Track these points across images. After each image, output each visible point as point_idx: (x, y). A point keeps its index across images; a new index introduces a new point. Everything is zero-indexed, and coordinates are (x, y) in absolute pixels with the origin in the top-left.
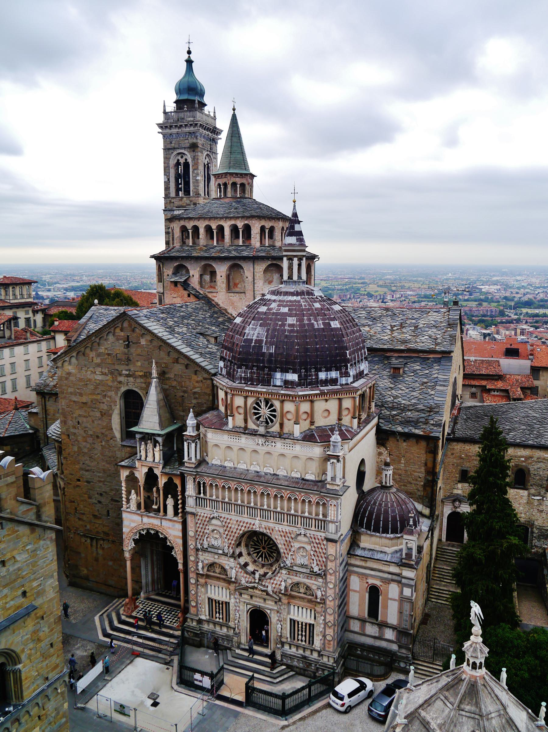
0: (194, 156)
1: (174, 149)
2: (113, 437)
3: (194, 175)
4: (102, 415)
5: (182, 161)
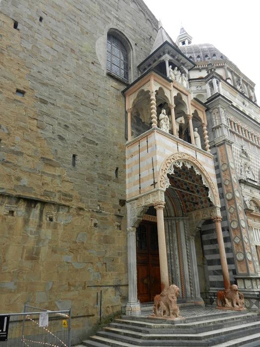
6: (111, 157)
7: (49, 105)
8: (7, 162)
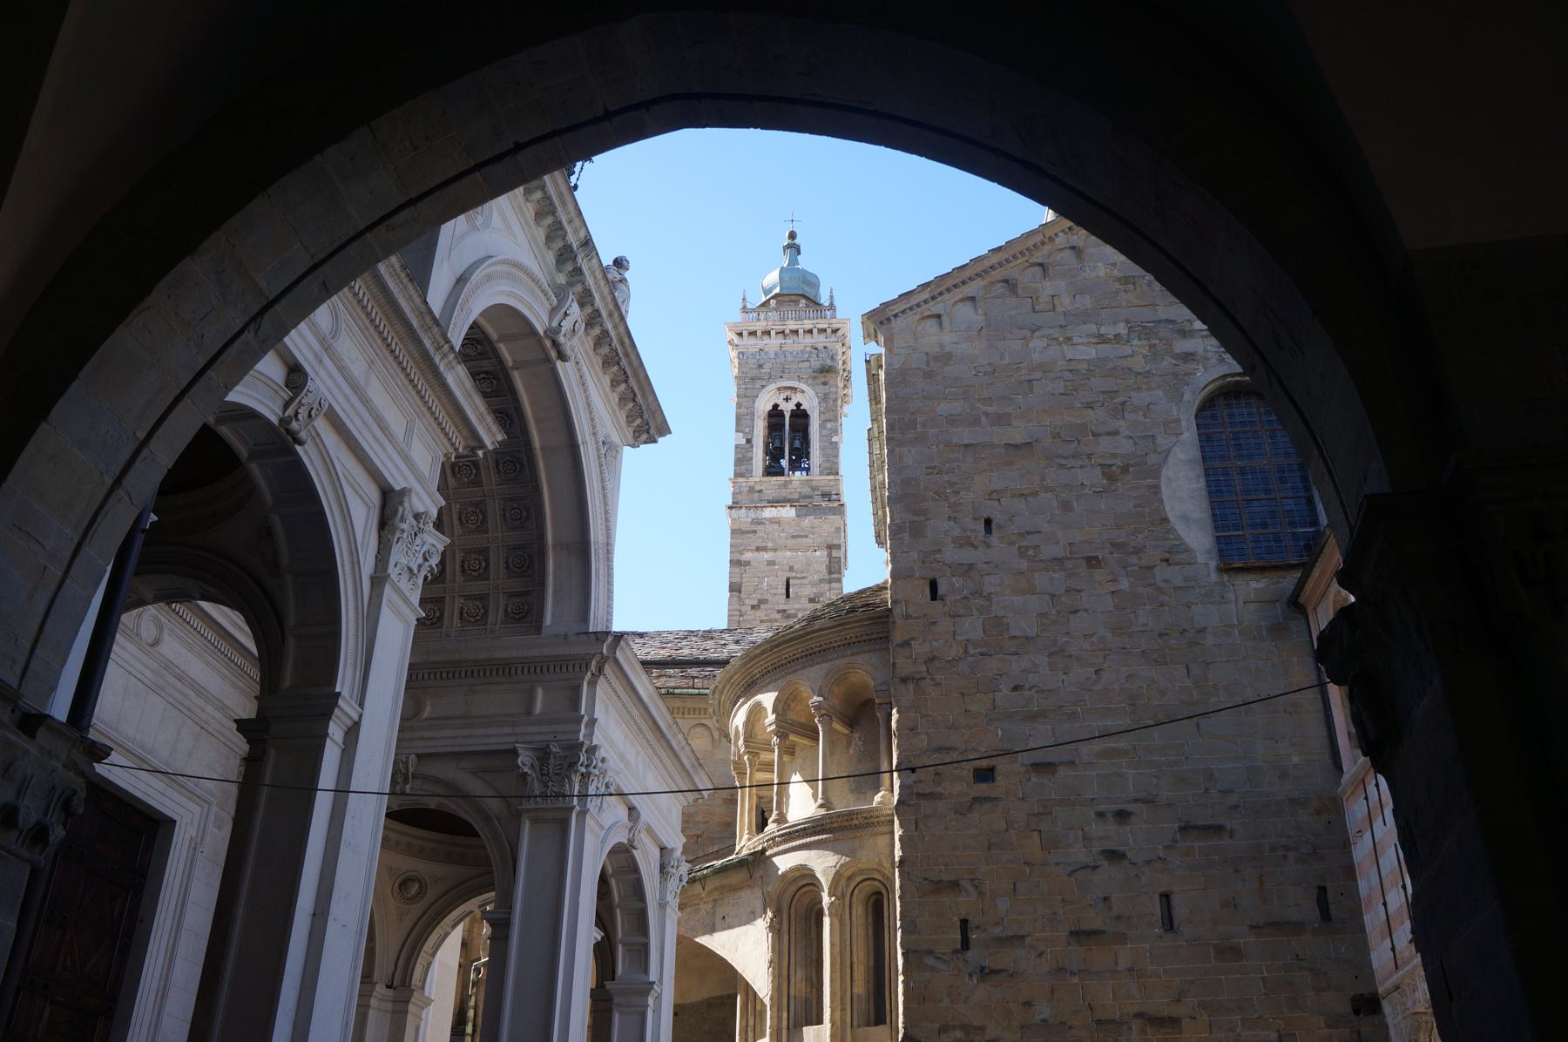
0: (826, 394)
1: (770, 378)
2: (1174, 554)
3: (825, 432)
4: (1111, 478)
5: (787, 408)
6: (1291, 855)
7: (1062, 772)
8: (994, 972)
